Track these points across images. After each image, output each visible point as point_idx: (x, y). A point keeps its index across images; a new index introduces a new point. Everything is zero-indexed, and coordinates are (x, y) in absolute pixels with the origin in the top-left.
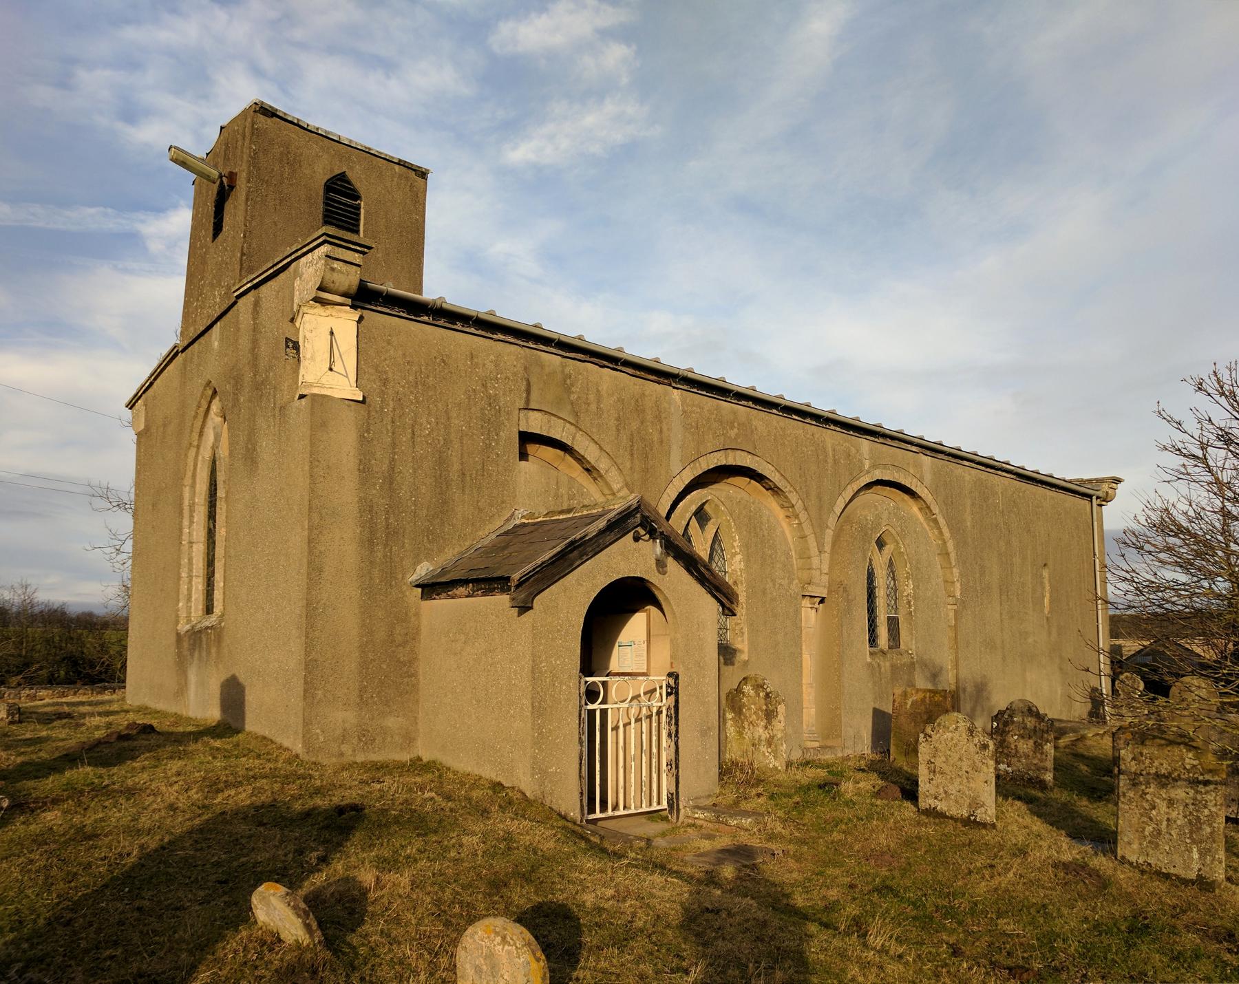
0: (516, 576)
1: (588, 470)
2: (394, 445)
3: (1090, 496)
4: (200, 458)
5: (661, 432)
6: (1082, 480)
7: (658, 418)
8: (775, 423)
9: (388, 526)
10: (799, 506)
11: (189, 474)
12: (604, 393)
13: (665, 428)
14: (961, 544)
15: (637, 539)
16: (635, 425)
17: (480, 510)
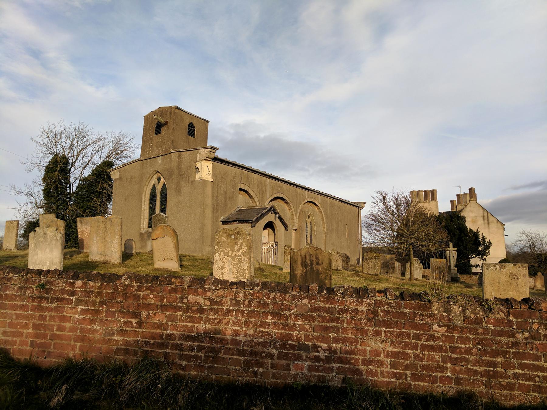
0: (254, 220)
1: (250, 197)
2: (218, 191)
3: (358, 207)
4: (148, 188)
5: (265, 188)
6: (356, 202)
9: (216, 208)
10: (292, 207)
11: (144, 192)
14: (327, 218)
15: (272, 213)
16: (260, 187)
17: (232, 205)
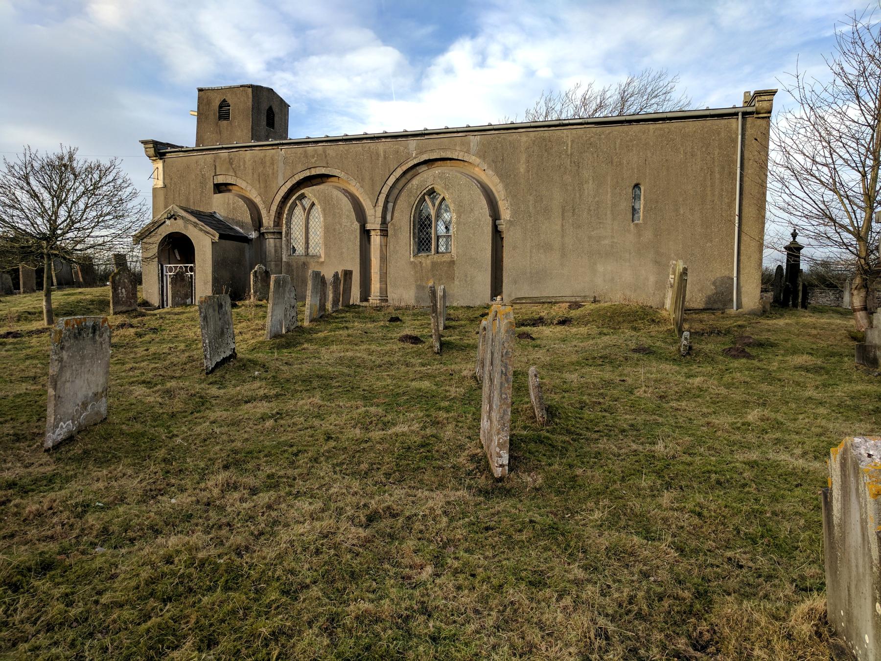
5: (273, 169)
7: (273, 164)
8: (342, 148)
12: (247, 161)
13: (275, 167)
16: (260, 170)
